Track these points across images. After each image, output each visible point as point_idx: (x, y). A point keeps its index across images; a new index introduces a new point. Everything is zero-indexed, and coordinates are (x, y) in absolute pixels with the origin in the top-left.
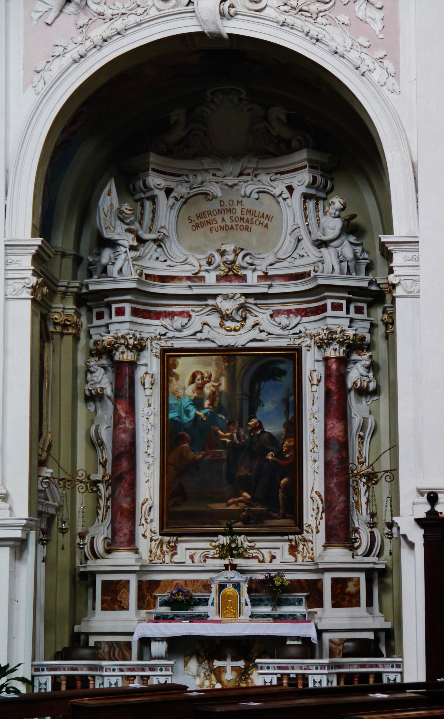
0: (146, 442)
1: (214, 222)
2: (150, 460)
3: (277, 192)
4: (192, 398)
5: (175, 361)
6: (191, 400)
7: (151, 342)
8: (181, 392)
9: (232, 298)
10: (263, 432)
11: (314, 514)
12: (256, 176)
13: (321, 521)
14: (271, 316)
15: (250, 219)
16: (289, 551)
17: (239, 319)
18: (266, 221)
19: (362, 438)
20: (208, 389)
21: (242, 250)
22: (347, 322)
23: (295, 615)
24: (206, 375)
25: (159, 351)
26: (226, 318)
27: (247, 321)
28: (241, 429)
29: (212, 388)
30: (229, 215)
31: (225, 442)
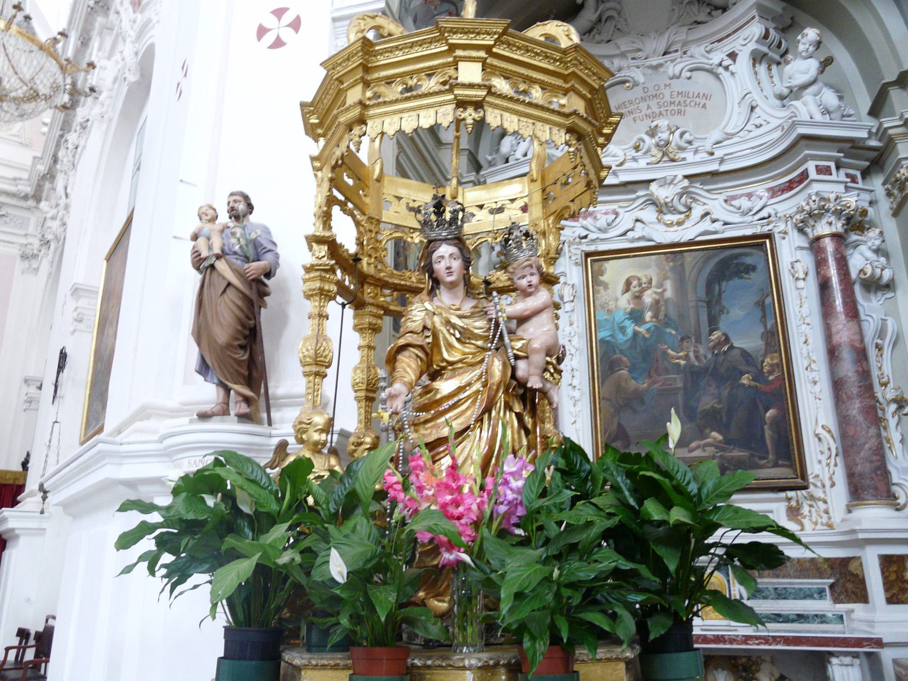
0: (570, 372)
1: (638, 111)
2: (576, 394)
3: (716, 61)
4: (628, 310)
5: (602, 266)
6: (626, 313)
7: (569, 247)
8: (612, 305)
9: (671, 183)
10: (732, 347)
11: (823, 458)
12: (685, 53)
13: (835, 468)
14: (726, 201)
15: (682, 101)
16: (787, 516)
17: (683, 209)
18: (703, 101)
19: (879, 348)
20: (648, 298)
21: (678, 128)
22: (841, 188)
23: (824, 616)
24: (644, 280)
25: (579, 257)
26: (664, 210)
27: (693, 212)
28: (699, 345)
29: (655, 296)
30: (655, 101)
31: (678, 364)
